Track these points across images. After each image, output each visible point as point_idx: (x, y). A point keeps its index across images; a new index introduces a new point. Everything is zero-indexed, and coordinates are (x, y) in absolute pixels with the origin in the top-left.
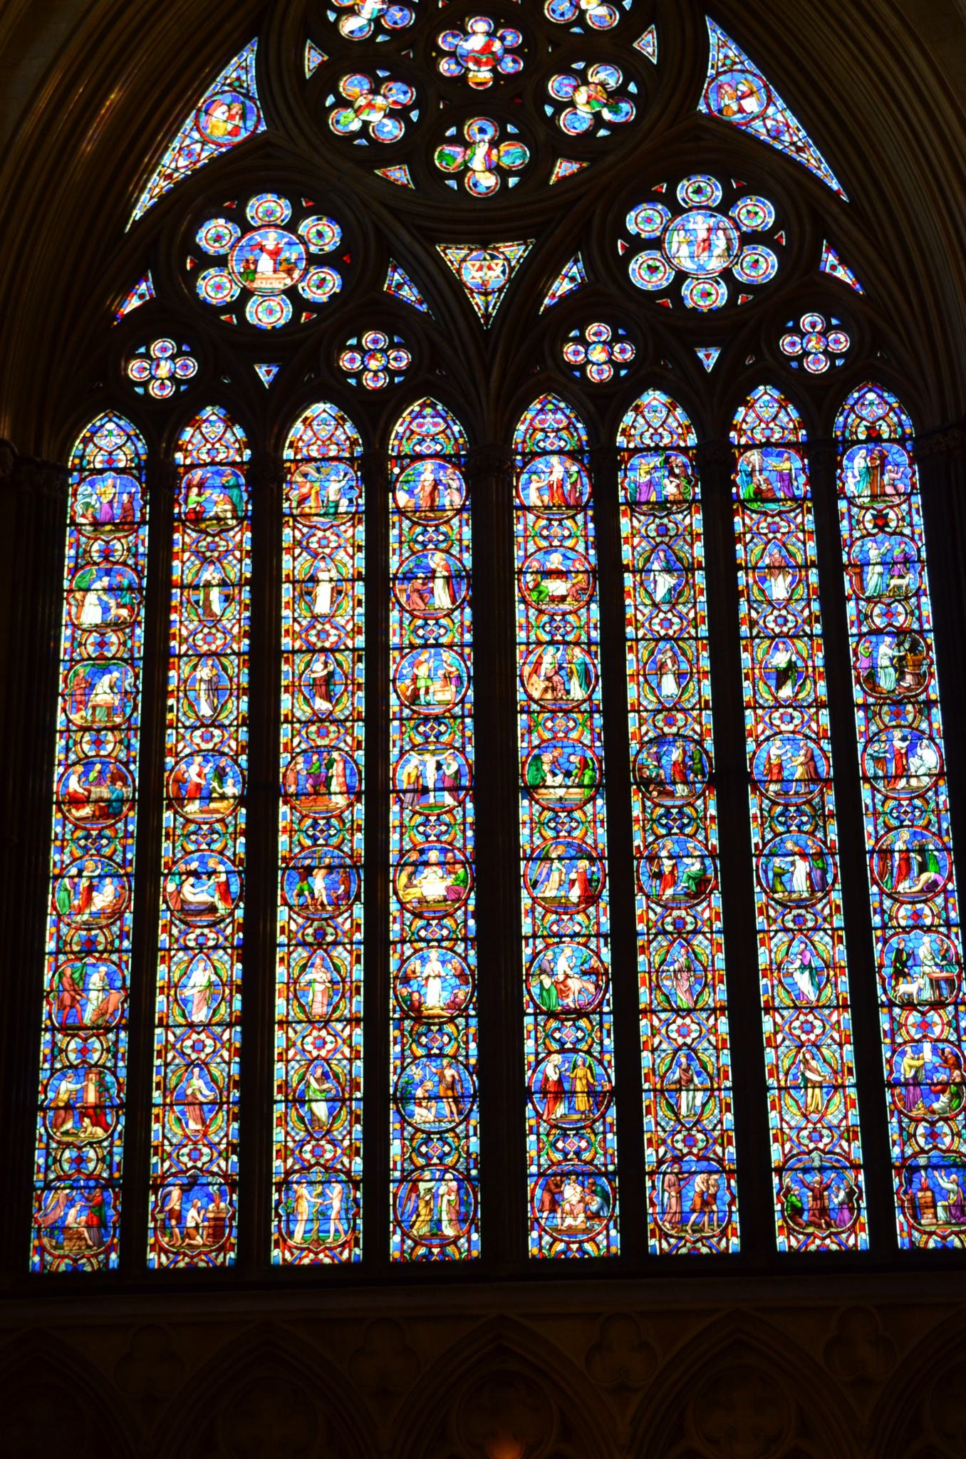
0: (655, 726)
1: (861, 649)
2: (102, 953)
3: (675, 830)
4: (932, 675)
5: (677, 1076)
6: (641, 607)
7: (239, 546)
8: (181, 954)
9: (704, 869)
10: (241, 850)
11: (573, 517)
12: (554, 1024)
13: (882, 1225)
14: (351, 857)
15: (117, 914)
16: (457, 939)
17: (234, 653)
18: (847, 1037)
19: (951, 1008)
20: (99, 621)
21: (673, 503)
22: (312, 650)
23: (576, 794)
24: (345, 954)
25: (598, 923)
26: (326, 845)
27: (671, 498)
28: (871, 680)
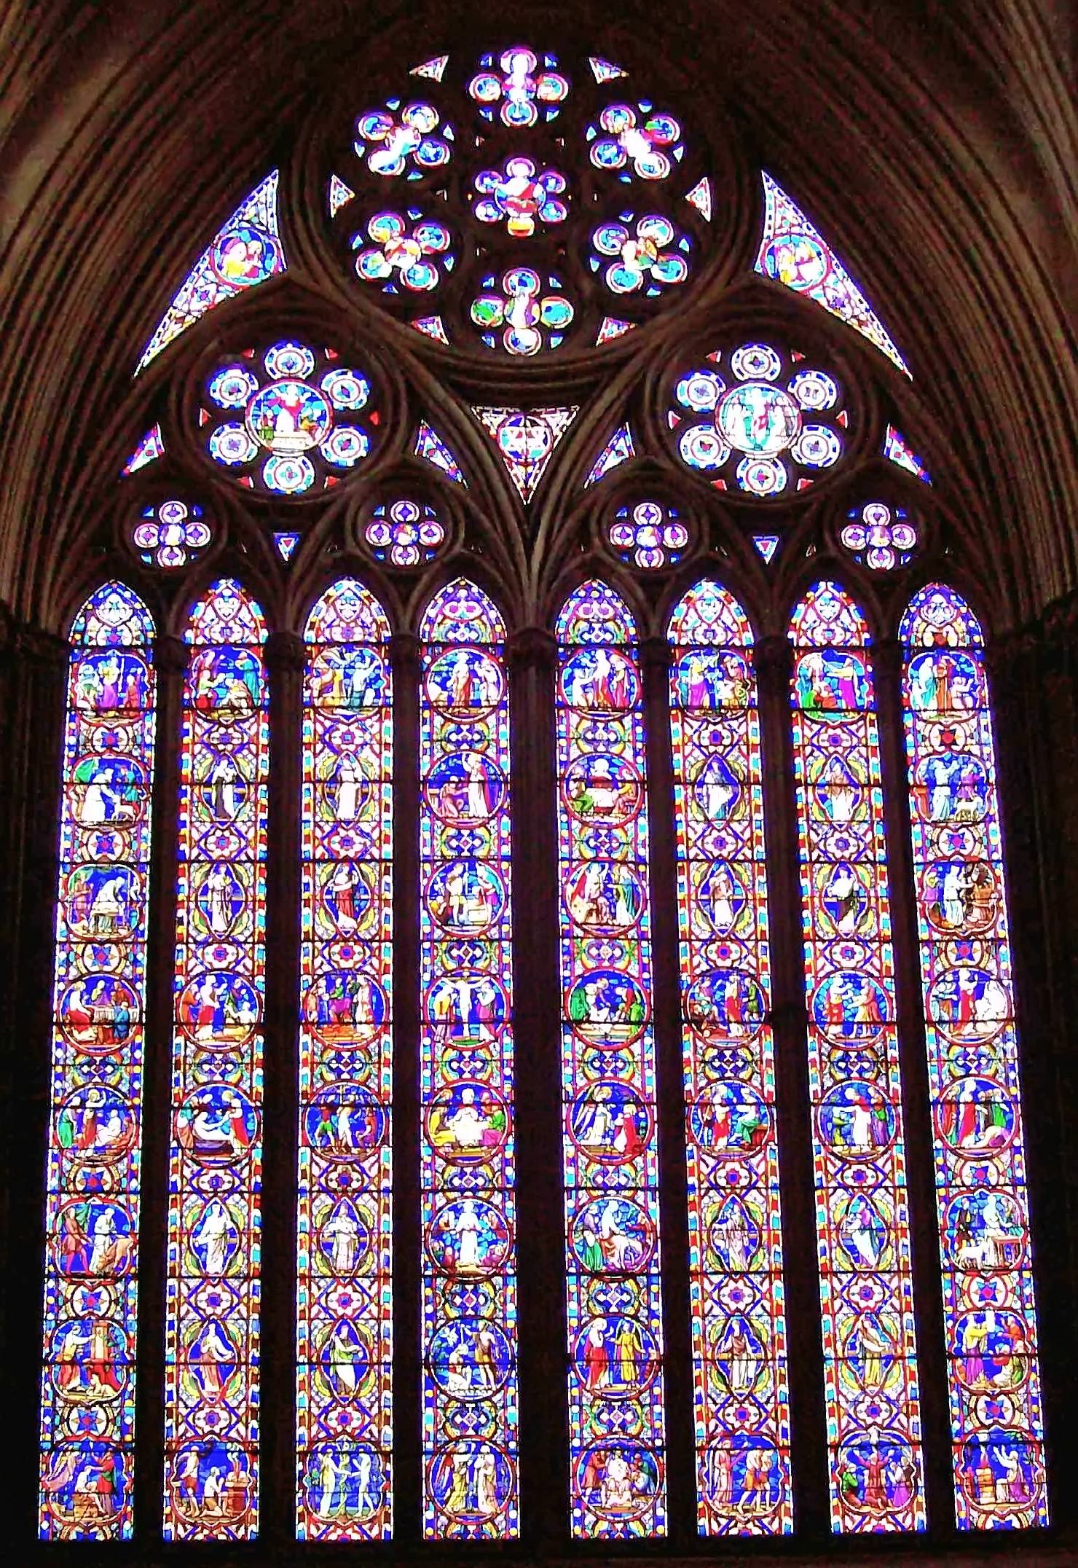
0: (708, 959)
1: (926, 878)
2: (108, 1193)
3: (729, 1074)
4: (1000, 909)
5: (729, 1345)
6: (693, 824)
8: (194, 1197)
10: (259, 1086)
11: (620, 720)
12: (597, 1285)
14: (378, 1094)
16: (494, 1189)
17: (249, 860)
18: (908, 1304)
19: (1015, 1274)
20: (102, 818)
21: (727, 708)
22: (333, 859)
23: (622, 1032)
24: (372, 1203)
25: (646, 1176)
26: (351, 1080)
27: (725, 703)
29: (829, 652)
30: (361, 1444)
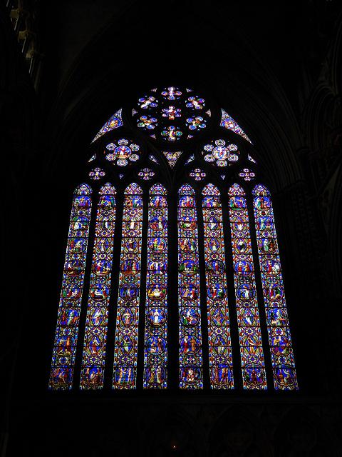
7: (113, 213)
9: (223, 291)
13: (270, 383)
15: (77, 297)
28: (262, 249)
29: (236, 197)
30: (129, 365)
